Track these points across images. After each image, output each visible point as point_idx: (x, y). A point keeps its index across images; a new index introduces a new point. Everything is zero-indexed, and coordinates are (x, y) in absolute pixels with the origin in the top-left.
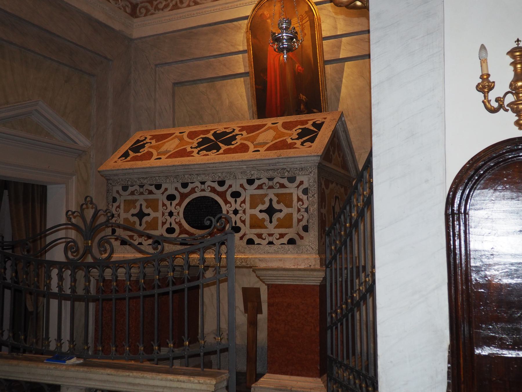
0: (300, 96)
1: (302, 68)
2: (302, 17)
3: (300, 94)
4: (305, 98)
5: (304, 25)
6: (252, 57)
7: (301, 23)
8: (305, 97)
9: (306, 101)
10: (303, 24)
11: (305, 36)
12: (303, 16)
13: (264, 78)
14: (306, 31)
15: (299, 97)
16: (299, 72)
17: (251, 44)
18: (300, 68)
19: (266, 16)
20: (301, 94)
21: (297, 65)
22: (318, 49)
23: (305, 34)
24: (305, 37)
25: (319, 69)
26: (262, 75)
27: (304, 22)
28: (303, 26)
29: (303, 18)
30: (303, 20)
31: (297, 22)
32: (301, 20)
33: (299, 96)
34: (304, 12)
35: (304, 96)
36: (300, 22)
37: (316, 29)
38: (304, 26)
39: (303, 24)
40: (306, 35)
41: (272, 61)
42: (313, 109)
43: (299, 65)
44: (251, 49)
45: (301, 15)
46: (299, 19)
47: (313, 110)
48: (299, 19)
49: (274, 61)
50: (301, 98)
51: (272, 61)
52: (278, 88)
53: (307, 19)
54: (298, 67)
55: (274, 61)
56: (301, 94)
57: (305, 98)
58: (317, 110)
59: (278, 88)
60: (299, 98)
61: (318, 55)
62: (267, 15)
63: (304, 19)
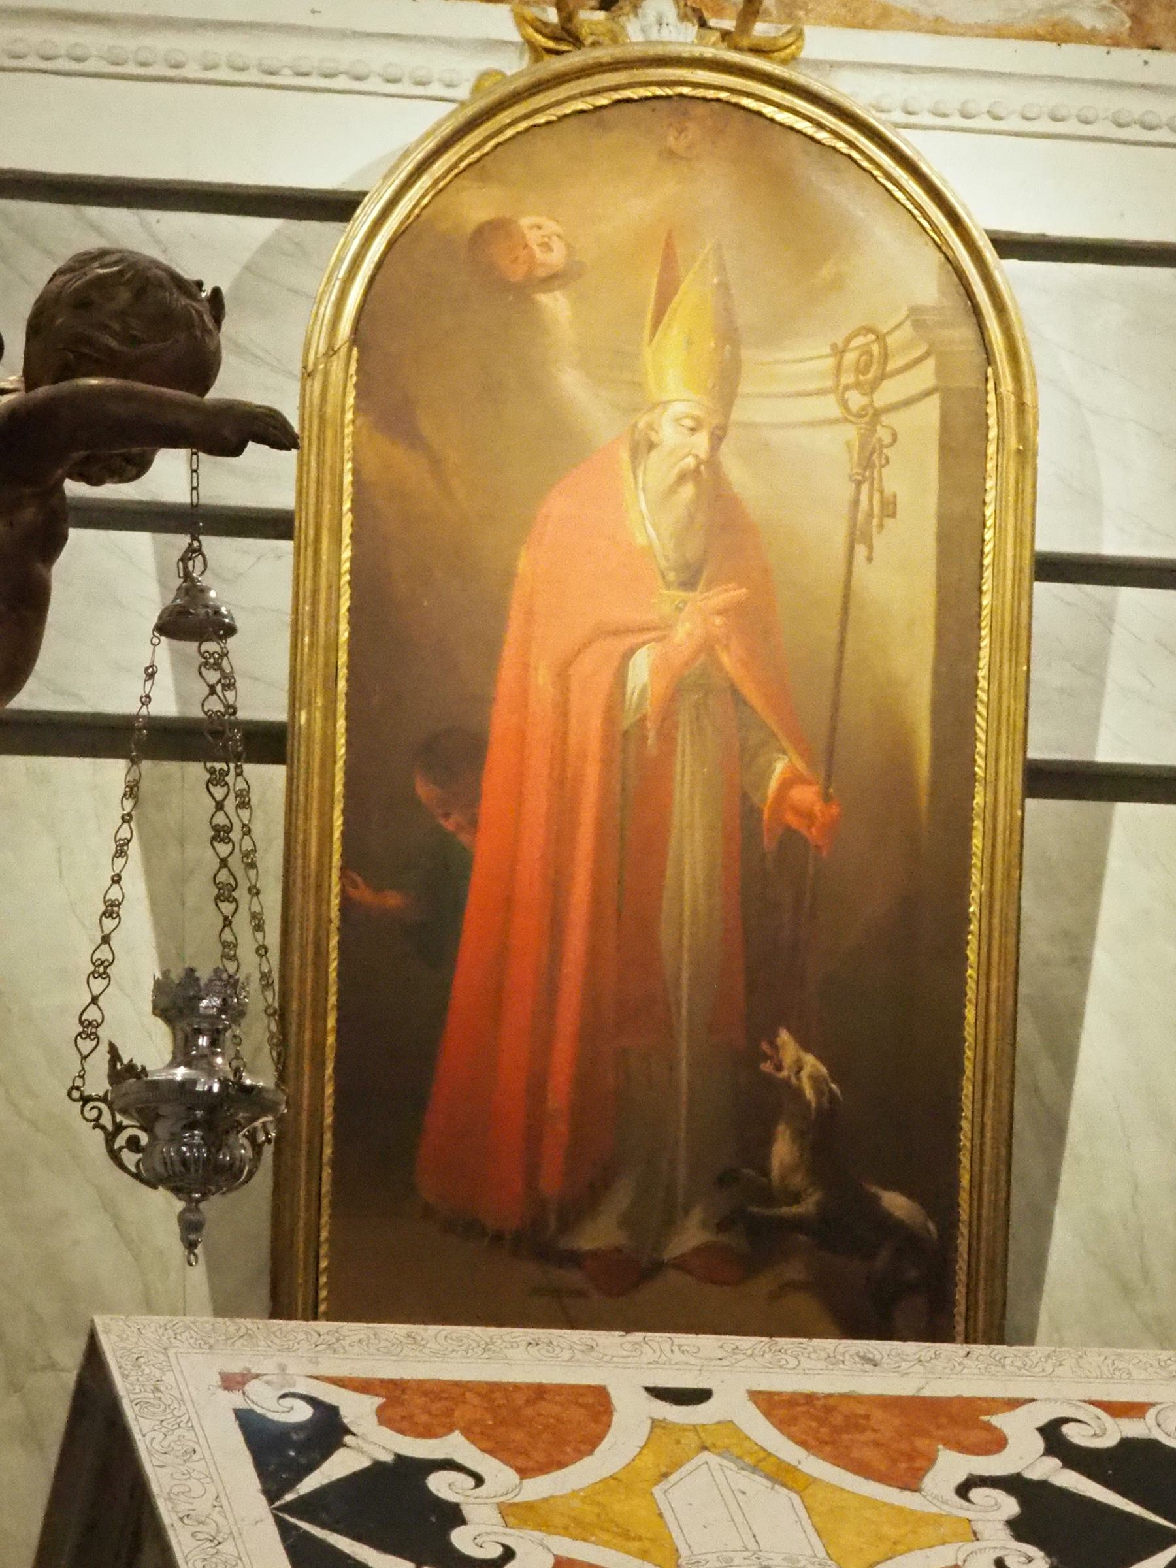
0: (776, 1048)
1: (826, 798)
2: (875, 349)
3: (776, 1035)
4: (815, 1079)
5: (885, 419)
6: (345, 603)
7: (856, 400)
8: (824, 1070)
9: (826, 1104)
10: (877, 414)
11: (888, 522)
12: (890, 340)
13: (449, 825)
14: (894, 480)
15: (766, 1057)
16: (789, 829)
17: (348, 478)
18: (806, 795)
19: (532, 256)
20: (784, 1036)
21: (780, 767)
22: (983, 663)
23: (889, 508)
24: (881, 526)
25: (977, 842)
26: (424, 790)
27: (889, 392)
28: (873, 431)
29: (885, 357)
30: (883, 376)
31: (829, 383)
32: (865, 371)
33: (765, 1046)
34: (904, 312)
35: (810, 1062)
36: (857, 385)
37: (990, 483)
38: (883, 434)
39: (877, 414)
40: (893, 515)
41: (542, 677)
42: (875, 1189)
43: (800, 765)
44: (347, 529)
45: (869, 330)
46: (850, 357)
47: (876, 1199)
48: (850, 357)
49: (562, 675)
50: (779, 1068)
51: (542, 677)
52: (576, 942)
53: (925, 376)
54: (787, 784)
55: (562, 675)
56: (784, 1036)
57: (815, 1079)
58: (910, 1196)
59: (576, 942)
60: (767, 1067)
61: (981, 709)
62: (546, 247)
63: (891, 366)
